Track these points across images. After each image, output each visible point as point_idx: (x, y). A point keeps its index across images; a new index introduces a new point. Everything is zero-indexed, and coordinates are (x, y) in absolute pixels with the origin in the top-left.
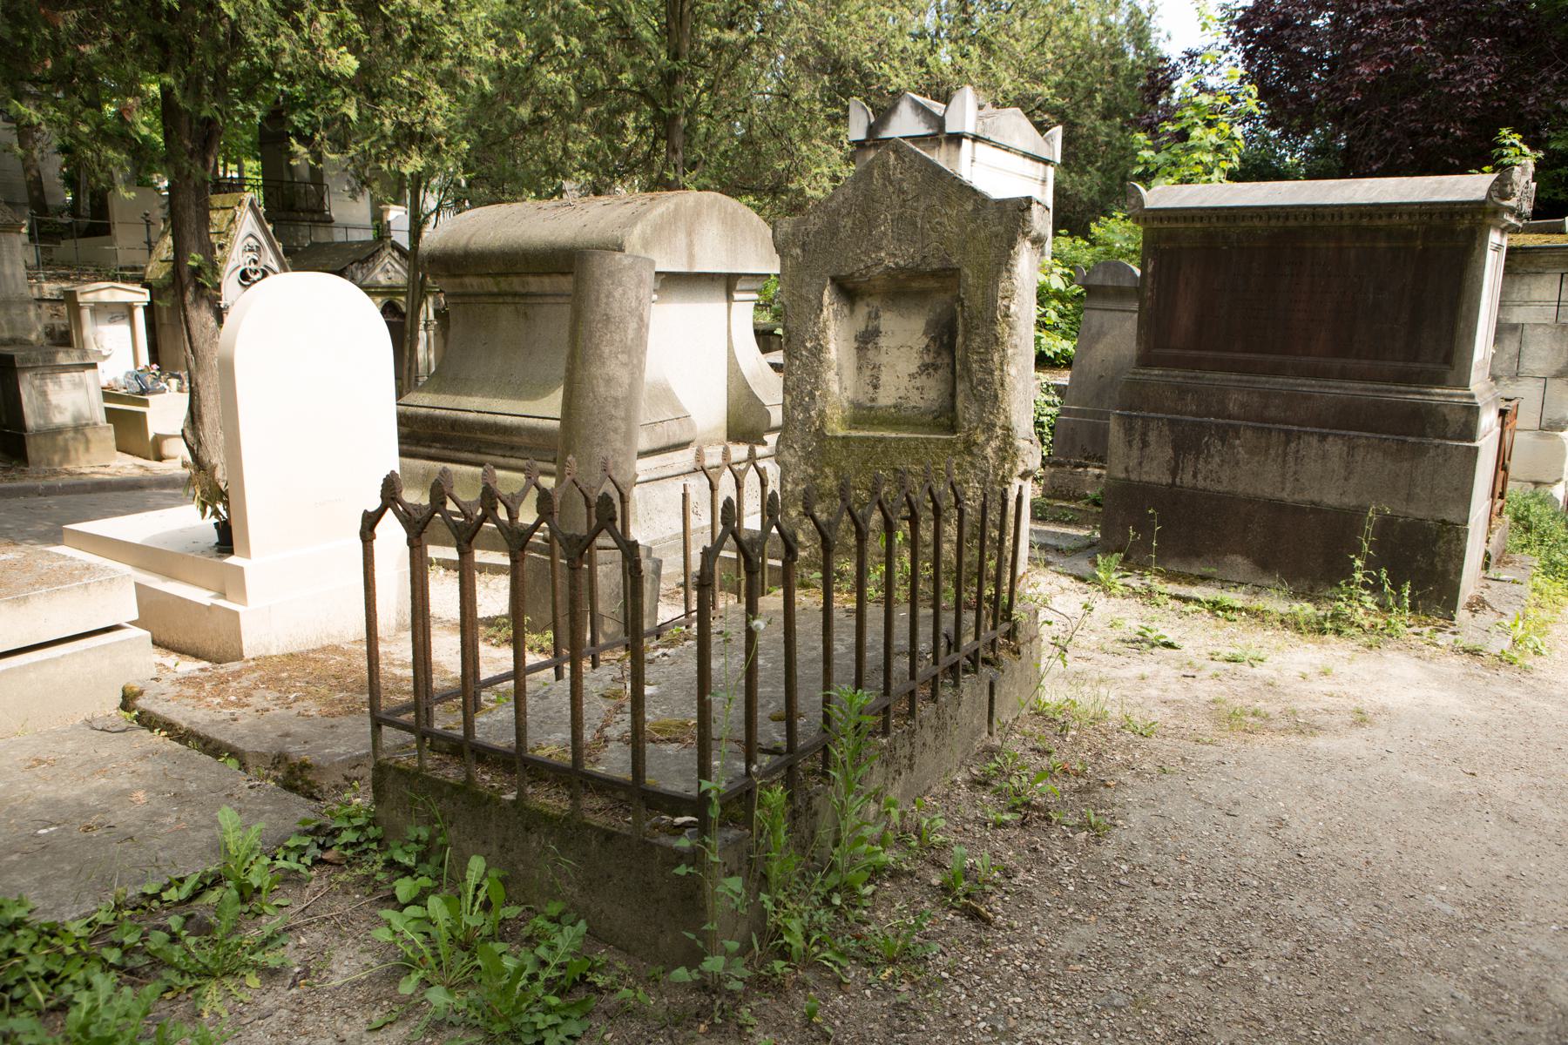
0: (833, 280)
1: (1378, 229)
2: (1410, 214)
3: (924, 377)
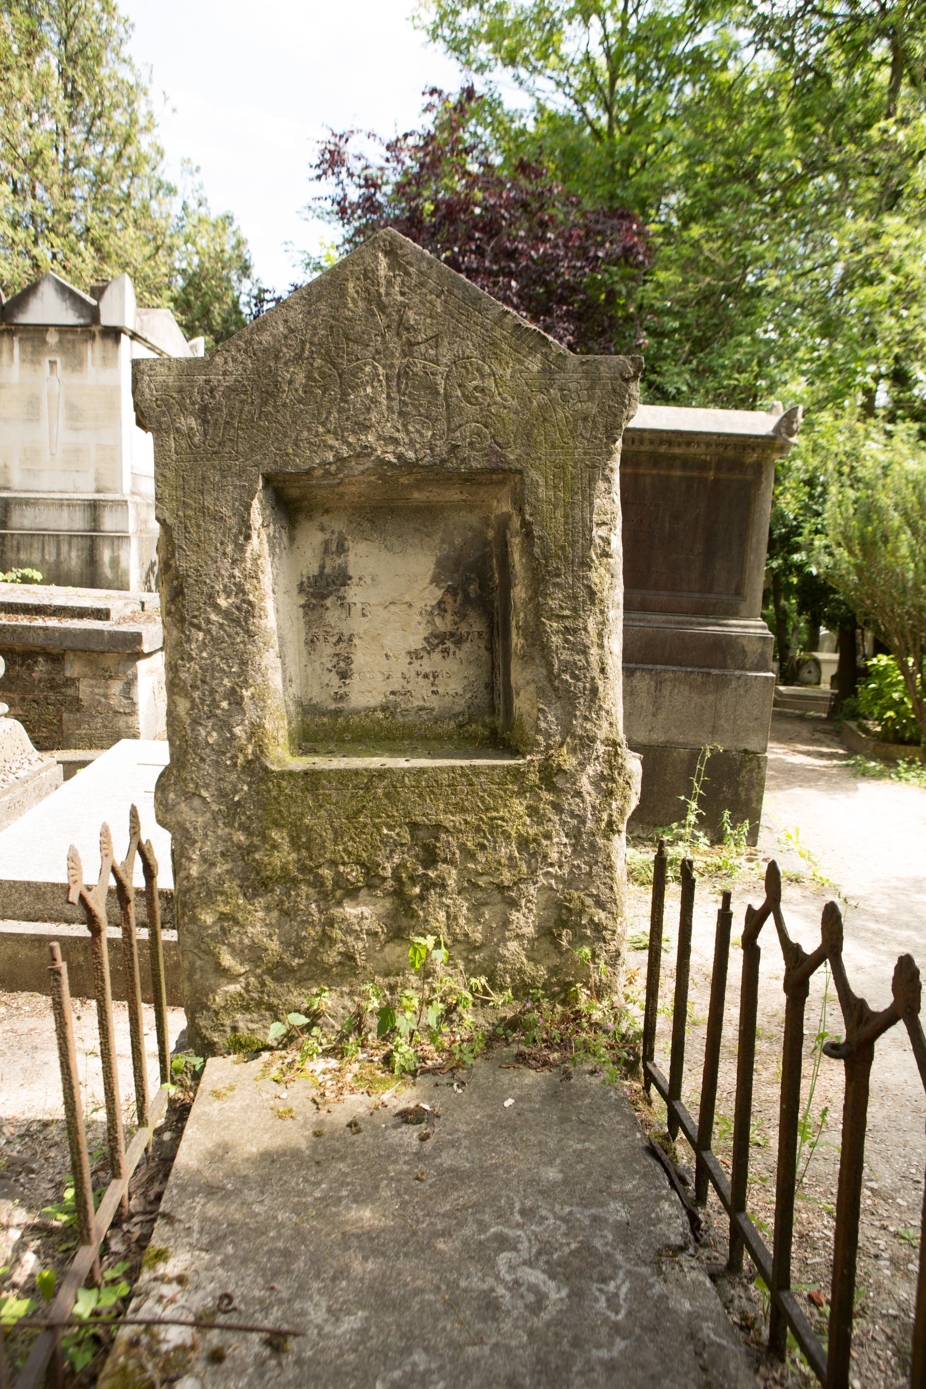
0: (268, 480)
1: (674, 457)
2: (708, 445)
3: (437, 656)
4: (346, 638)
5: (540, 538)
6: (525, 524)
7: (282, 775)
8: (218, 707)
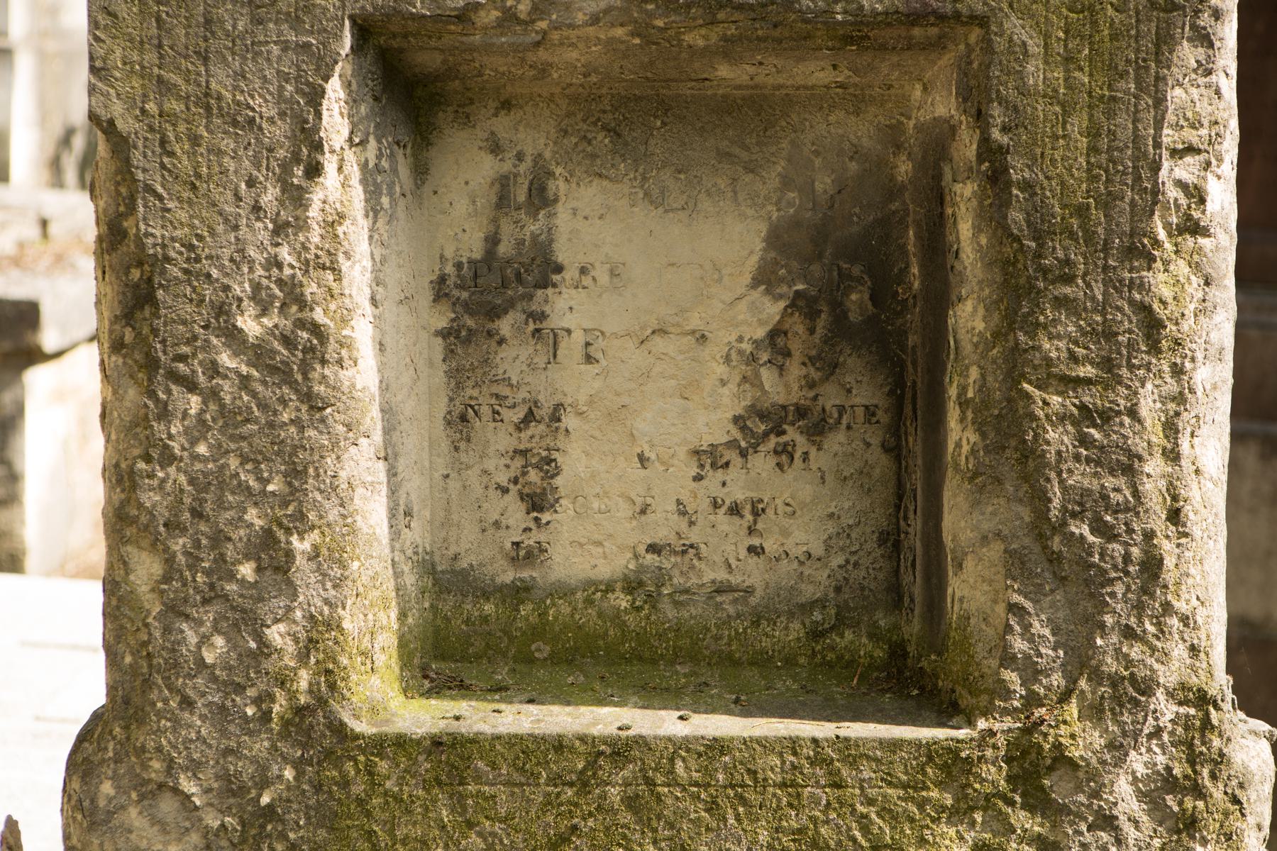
0: (364, 31)
3: (762, 463)
4: (544, 412)
5: (1027, 186)
6: (988, 150)
7: (379, 745)
8: (231, 576)
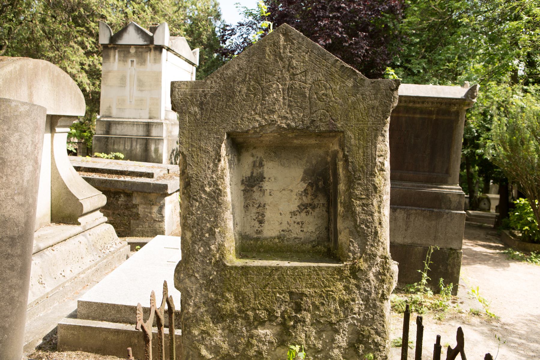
0: (229, 135)
1: (416, 109)
2: (432, 103)
3: (303, 214)
4: (262, 205)
5: (352, 162)
6: (345, 156)
7: (232, 268)
8: (204, 236)
